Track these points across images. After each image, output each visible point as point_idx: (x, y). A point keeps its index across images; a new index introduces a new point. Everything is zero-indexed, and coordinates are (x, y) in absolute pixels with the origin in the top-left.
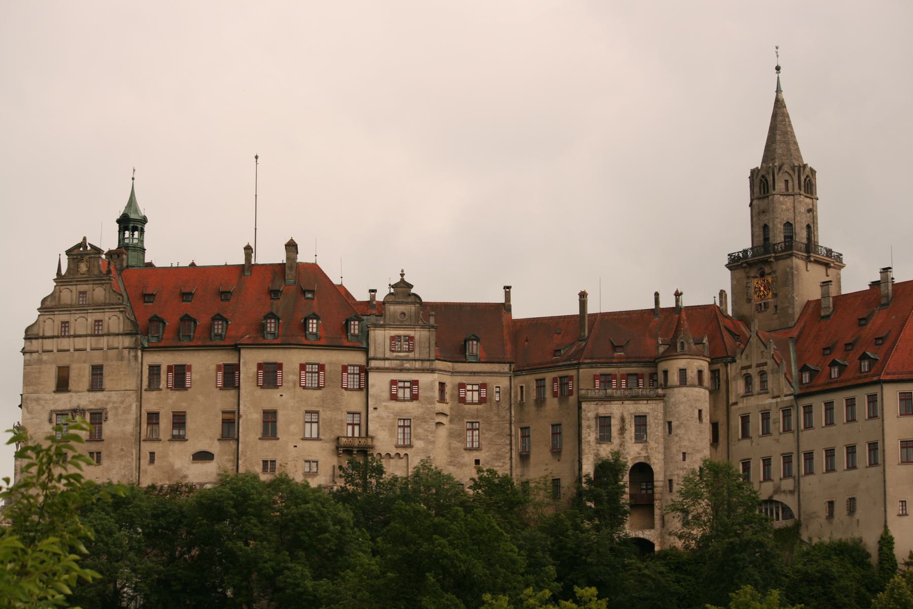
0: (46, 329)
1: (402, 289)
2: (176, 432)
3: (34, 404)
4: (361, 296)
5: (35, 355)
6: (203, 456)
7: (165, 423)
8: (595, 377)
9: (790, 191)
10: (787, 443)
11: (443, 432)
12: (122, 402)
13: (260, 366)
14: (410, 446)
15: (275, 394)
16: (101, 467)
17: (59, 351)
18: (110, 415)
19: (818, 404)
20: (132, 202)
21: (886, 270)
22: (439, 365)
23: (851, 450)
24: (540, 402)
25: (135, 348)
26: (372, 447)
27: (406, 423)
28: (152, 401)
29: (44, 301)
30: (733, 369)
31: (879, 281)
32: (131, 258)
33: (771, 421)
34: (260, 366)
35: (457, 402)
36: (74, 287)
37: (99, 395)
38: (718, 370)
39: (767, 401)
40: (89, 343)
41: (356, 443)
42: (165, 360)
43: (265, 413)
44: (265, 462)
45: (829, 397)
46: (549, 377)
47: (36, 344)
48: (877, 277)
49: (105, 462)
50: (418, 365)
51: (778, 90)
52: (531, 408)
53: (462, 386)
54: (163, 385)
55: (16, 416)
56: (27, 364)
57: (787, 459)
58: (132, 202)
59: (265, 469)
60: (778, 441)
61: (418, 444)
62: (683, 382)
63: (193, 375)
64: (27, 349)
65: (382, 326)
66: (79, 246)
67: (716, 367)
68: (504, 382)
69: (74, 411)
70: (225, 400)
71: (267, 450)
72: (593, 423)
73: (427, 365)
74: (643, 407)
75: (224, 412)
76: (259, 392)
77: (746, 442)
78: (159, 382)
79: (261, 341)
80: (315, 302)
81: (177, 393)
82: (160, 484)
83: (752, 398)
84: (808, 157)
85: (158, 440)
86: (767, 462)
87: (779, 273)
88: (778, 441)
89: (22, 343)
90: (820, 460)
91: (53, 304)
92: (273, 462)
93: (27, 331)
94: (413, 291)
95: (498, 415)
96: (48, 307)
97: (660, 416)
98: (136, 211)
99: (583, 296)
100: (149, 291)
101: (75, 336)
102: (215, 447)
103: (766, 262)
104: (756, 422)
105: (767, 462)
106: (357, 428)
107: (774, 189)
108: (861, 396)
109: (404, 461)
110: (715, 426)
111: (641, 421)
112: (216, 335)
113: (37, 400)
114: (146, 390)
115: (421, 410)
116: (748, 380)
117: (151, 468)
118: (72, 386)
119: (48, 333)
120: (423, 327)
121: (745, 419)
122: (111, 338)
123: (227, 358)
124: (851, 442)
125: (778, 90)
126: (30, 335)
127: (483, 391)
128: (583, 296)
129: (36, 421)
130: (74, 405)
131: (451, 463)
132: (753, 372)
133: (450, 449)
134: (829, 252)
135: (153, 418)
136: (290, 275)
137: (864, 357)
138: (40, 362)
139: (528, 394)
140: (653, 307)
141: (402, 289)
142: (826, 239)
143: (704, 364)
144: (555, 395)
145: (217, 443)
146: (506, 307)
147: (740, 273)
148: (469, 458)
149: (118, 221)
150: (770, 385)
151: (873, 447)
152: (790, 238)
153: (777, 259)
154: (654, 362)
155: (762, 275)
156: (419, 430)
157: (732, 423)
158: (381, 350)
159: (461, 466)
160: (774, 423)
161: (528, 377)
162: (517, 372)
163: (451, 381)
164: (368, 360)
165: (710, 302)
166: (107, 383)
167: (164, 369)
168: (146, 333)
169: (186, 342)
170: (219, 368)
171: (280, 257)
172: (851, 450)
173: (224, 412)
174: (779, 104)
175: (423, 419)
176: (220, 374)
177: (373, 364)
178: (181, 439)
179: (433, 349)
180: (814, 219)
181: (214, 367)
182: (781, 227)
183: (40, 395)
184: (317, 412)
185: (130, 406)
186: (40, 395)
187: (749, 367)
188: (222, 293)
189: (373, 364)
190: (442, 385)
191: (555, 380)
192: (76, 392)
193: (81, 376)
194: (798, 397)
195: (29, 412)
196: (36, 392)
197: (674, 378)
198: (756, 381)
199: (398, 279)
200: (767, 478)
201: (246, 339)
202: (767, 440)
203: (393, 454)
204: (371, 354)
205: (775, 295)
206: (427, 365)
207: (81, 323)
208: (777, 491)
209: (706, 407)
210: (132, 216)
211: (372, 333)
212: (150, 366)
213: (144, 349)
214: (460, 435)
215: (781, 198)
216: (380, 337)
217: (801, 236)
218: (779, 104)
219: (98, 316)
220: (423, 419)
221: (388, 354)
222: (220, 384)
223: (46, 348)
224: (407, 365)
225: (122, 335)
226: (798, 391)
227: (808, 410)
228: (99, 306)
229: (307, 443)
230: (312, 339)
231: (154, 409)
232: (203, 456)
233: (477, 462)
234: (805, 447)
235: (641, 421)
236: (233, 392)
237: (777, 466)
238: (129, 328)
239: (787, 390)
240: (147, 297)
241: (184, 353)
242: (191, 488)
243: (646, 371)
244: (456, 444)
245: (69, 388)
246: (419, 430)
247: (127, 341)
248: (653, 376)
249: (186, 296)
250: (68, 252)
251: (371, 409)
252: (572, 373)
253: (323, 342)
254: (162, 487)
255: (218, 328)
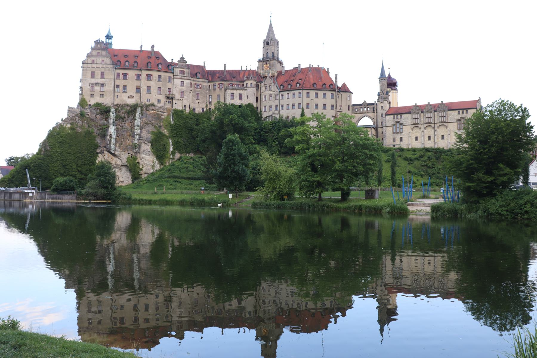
0: (88, 61)
1: (182, 60)
2: (124, 91)
3: (85, 81)
4: (169, 60)
5: (85, 68)
6: (131, 97)
7: (121, 88)
8: (229, 84)
9: (274, 45)
10: (277, 103)
11: (191, 95)
12: (110, 82)
13: (147, 75)
14: (183, 98)
15: (151, 82)
16: (103, 98)
17: (92, 67)
18: (106, 85)
19: (285, 93)
20: (109, 32)
21: (300, 65)
22: (191, 78)
23: (294, 105)
24: (215, 89)
25: (113, 68)
26: (174, 97)
27: (182, 92)
28: (118, 82)
29: (87, 54)
30: (262, 85)
31: (298, 68)
32: (109, 46)
33: (272, 97)
34: (147, 75)
35: (194, 88)
36: (96, 51)
37: (103, 80)
38: (258, 85)
39: (271, 92)
40: (100, 66)
41: (170, 96)
42: (121, 72)
43: (148, 87)
44: (147, 99)
45: (288, 92)
46: (217, 83)
47: (85, 65)
48: (297, 66)
49: (105, 97)
50: (186, 78)
51: (271, 22)
52: (212, 91)
53: (195, 84)
54: (121, 78)
55: (80, 84)
56: (83, 70)
57: (276, 106)
58: (109, 32)
59: (147, 101)
60: (274, 102)
61: (185, 97)
62: (251, 87)
63: (129, 77)
64: (83, 66)
65: (177, 68)
66: (98, 40)
67: (258, 84)
68: (205, 84)
69: (96, 83)
70: (138, 83)
71: (148, 96)
72: (229, 94)
73: (188, 78)
74: (241, 92)
75: (137, 86)
76: (146, 81)
77: (265, 102)
78: (119, 77)
79: (147, 68)
80: (159, 61)
81: (124, 80)
82: (119, 103)
83: (267, 92)
84: (277, 38)
85: (119, 92)
86: (271, 107)
87: (271, 64)
88: (274, 102)
89: (81, 65)
90: (285, 107)
91: (90, 55)
92: (150, 99)
93: (83, 62)
94: (185, 60)
95: (204, 92)
96: (89, 56)
97: (245, 94)
98: (110, 34)
99: (225, 65)
100: (116, 54)
101: (96, 64)
102: (134, 95)
103: (268, 61)
104: (268, 96)
105: (271, 107)
106: (170, 92)
107: (270, 44)
108: (297, 92)
109: (182, 101)
110: (257, 98)
111: (241, 95)
112: (135, 66)
113: (86, 80)
114: (116, 79)
115: (186, 89)
116: (266, 86)
117: (117, 99)
118: (95, 76)
119: (89, 63)
120: (187, 69)
121: (265, 96)
122: (107, 65)
123: (139, 72)
124: (294, 103)
125: (271, 22)
126: (84, 63)
127: (201, 86)
128: (225, 65)
129: (85, 85)
130: (96, 82)
131: (192, 103)
132: (268, 85)
133: (192, 99)
134: (281, 60)
135: (118, 86)
136: (153, 54)
137: (298, 83)
138: (86, 70)
139: (211, 87)
140: (241, 69)
141: (182, 60)
142: (281, 58)
143: (255, 83)
144: (219, 88)
145: (135, 94)
146: (204, 67)
147: (261, 63)
148: (197, 101)
149: (106, 36)
150: (272, 89)
151: (300, 104)
152: (273, 56)
153: (271, 60)
154: (243, 82)
155: (267, 64)
156: (186, 94)
157: (262, 97)
158: (177, 73)
159: (195, 103)
160: (273, 97)
161: (212, 83)
162: (209, 81)
163: (193, 83)
164: (174, 76)
165: (255, 69)
166: (105, 76)
167: (121, 74)
168: (116, 64)
169: (127, 67)
170: (136, 75)
171: (149, 49)
172: (294, 105)
173: (137, 86)
174: (271, 25)
175: (187, 91)
176: (136, 76)
177: (175, 77)
178: (126, 92)
179: (189, 74)
180: (278, 52)
181: (134, 74)
182: (271, 53)
183: (87, 79)
184: (161, 88)
185: (112, 83)
186: (87, 79)
187: (267, 84)
188: (135, 56)
189: (175, 77)
190: (191, 83)
191: (219, 84)
192: (97, 78)
193: (98, 74)
194: (280, 92)
195: (83, 83)
196: (86, 78)
197: (249, 85)
198: (268, 87)
199: (181, 57)
200: (270, 111)
201: (143, 68)
202: (271, 102)
203: (179, 99)
204: (174, 74)
205: (270, 69)
206: (188, 78)
207: (99, 60)
208: (274, 113)
209: (256, 92)
210: (110, 35)
211: (174, 69)
212: (117, 73)
213: (116, 69)
214: (195, 96)
215: (272, 47)
216: (177, 70)
217: (276, 55)
218: (271, 25)
219: (103, 59)
220: (187, 91)
221: (178, 75)
222: (136, 79)
223: (88, 66)
224: (183, 78)
225: (110, 64)
226: (280, 91)
227: (282, 95)
228: (103, 56)
229: (158, 95)
230: (160, 70)
231: (118, 84)
232: (131, 97)
233: (199, 103)
234: (281, 104)
235: (241, 95)
236: (139, 81)
237: (273, 108)
238: (111, 63)
239: (277, 90)
240: (115, 56)
241: (126, 70)
242: (128, 105)
243: (241, 83)
244: (194, 98)
245: (95, 77)
246: (186, 94)
247: (111, 66)
248: (243, 85)
249: (126, 56)
250: (95, 42)
251: (174, 88)
252: (224, 83)
253: (162, 70)
254: (120, 105)
255: (136, 65)
